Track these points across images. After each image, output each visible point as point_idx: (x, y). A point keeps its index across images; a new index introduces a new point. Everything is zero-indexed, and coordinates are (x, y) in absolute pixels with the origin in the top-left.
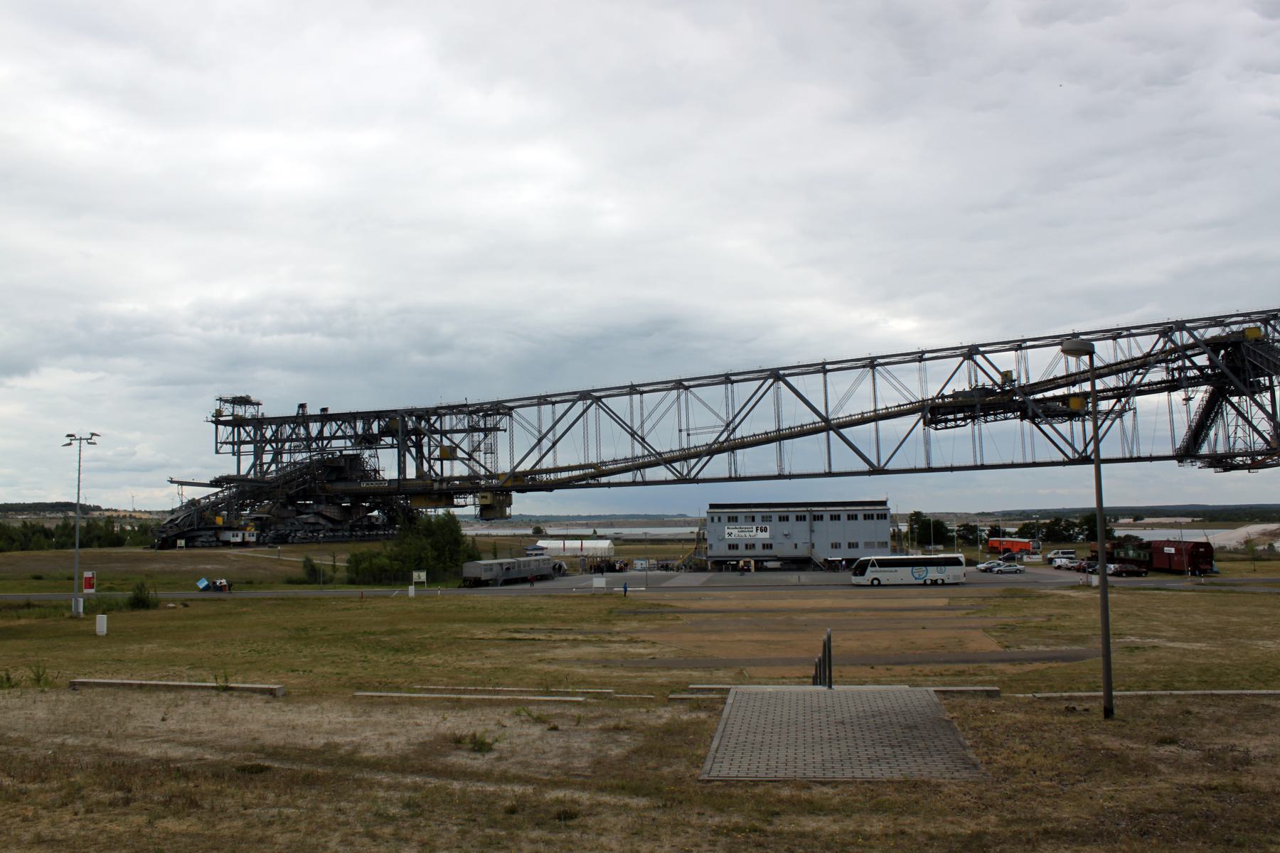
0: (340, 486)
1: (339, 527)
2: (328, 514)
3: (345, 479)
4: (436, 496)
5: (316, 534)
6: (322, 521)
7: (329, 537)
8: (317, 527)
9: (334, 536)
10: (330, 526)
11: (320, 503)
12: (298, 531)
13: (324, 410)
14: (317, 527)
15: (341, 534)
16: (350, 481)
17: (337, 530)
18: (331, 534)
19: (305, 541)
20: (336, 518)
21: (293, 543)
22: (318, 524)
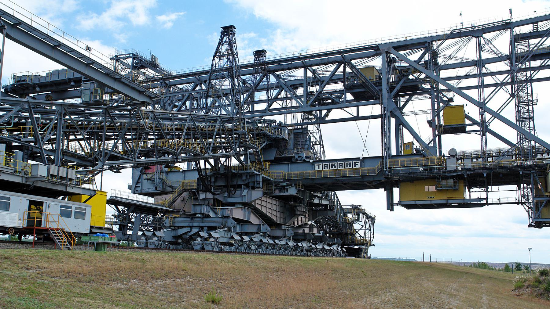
0: (283, 170)
1: (278, 233)
2: (264, 210)
3: (288, 160)
4: (451, 182)
5: (246, 238)
6: (254, 220)
7: (267, 247)
8: (248, 229)
9: (275, 245)
10: (265, 227)
11: (253, 188)
12: (214, 229)
13: (259, 54)
14: (248, 229)
15: (283, 242)
16: (297, 162)
17: (278, 238)
18: (271, 241)
19: (227, 248)
20: (274, 218)
21: (203, 249)
22: (248, 222)
